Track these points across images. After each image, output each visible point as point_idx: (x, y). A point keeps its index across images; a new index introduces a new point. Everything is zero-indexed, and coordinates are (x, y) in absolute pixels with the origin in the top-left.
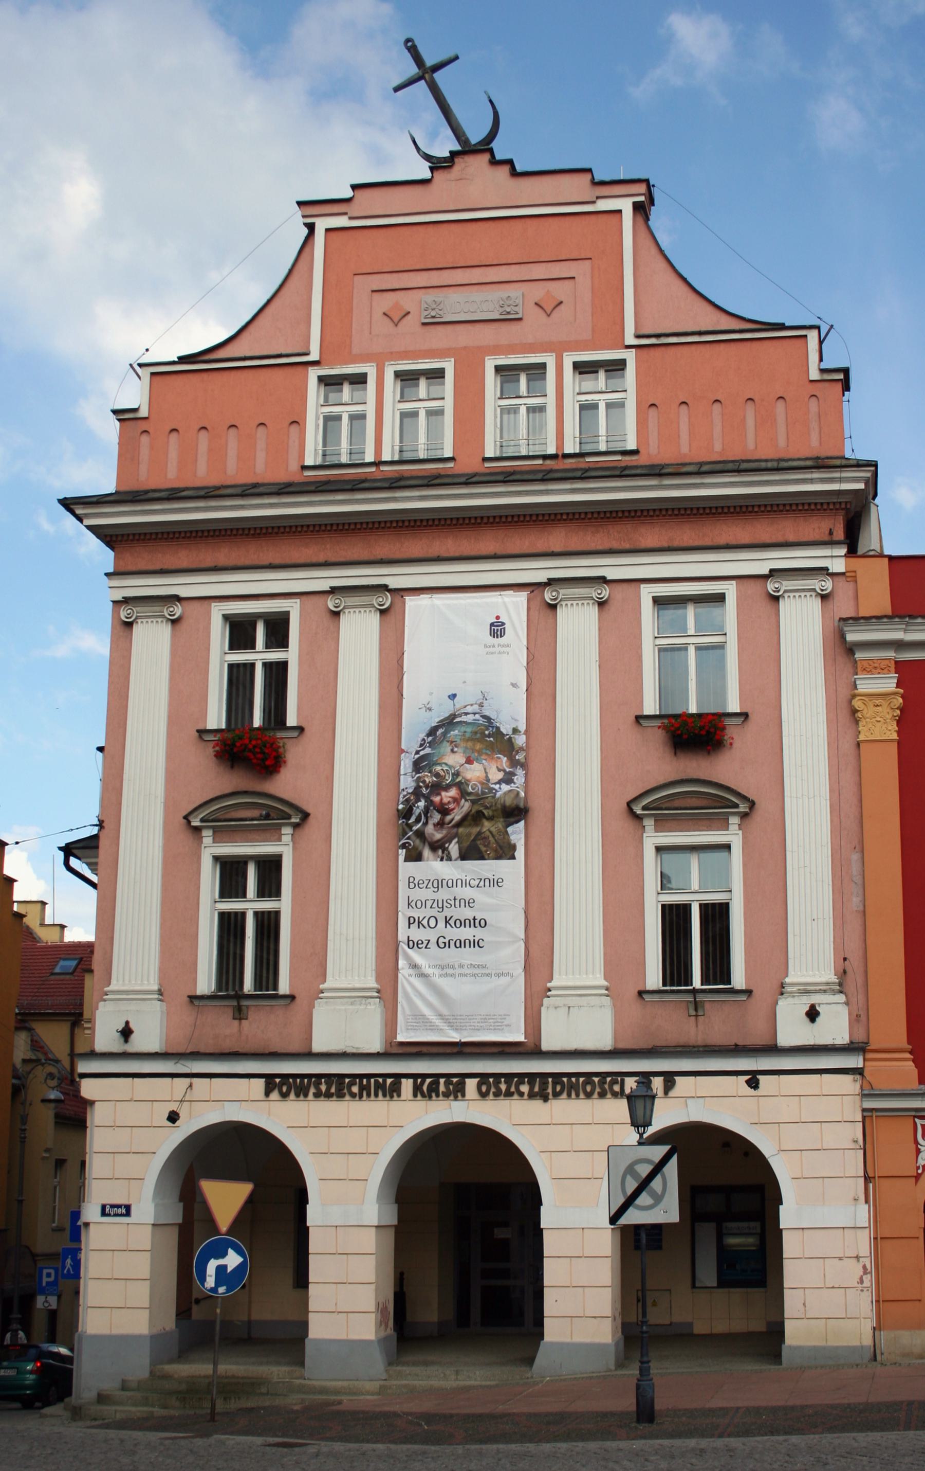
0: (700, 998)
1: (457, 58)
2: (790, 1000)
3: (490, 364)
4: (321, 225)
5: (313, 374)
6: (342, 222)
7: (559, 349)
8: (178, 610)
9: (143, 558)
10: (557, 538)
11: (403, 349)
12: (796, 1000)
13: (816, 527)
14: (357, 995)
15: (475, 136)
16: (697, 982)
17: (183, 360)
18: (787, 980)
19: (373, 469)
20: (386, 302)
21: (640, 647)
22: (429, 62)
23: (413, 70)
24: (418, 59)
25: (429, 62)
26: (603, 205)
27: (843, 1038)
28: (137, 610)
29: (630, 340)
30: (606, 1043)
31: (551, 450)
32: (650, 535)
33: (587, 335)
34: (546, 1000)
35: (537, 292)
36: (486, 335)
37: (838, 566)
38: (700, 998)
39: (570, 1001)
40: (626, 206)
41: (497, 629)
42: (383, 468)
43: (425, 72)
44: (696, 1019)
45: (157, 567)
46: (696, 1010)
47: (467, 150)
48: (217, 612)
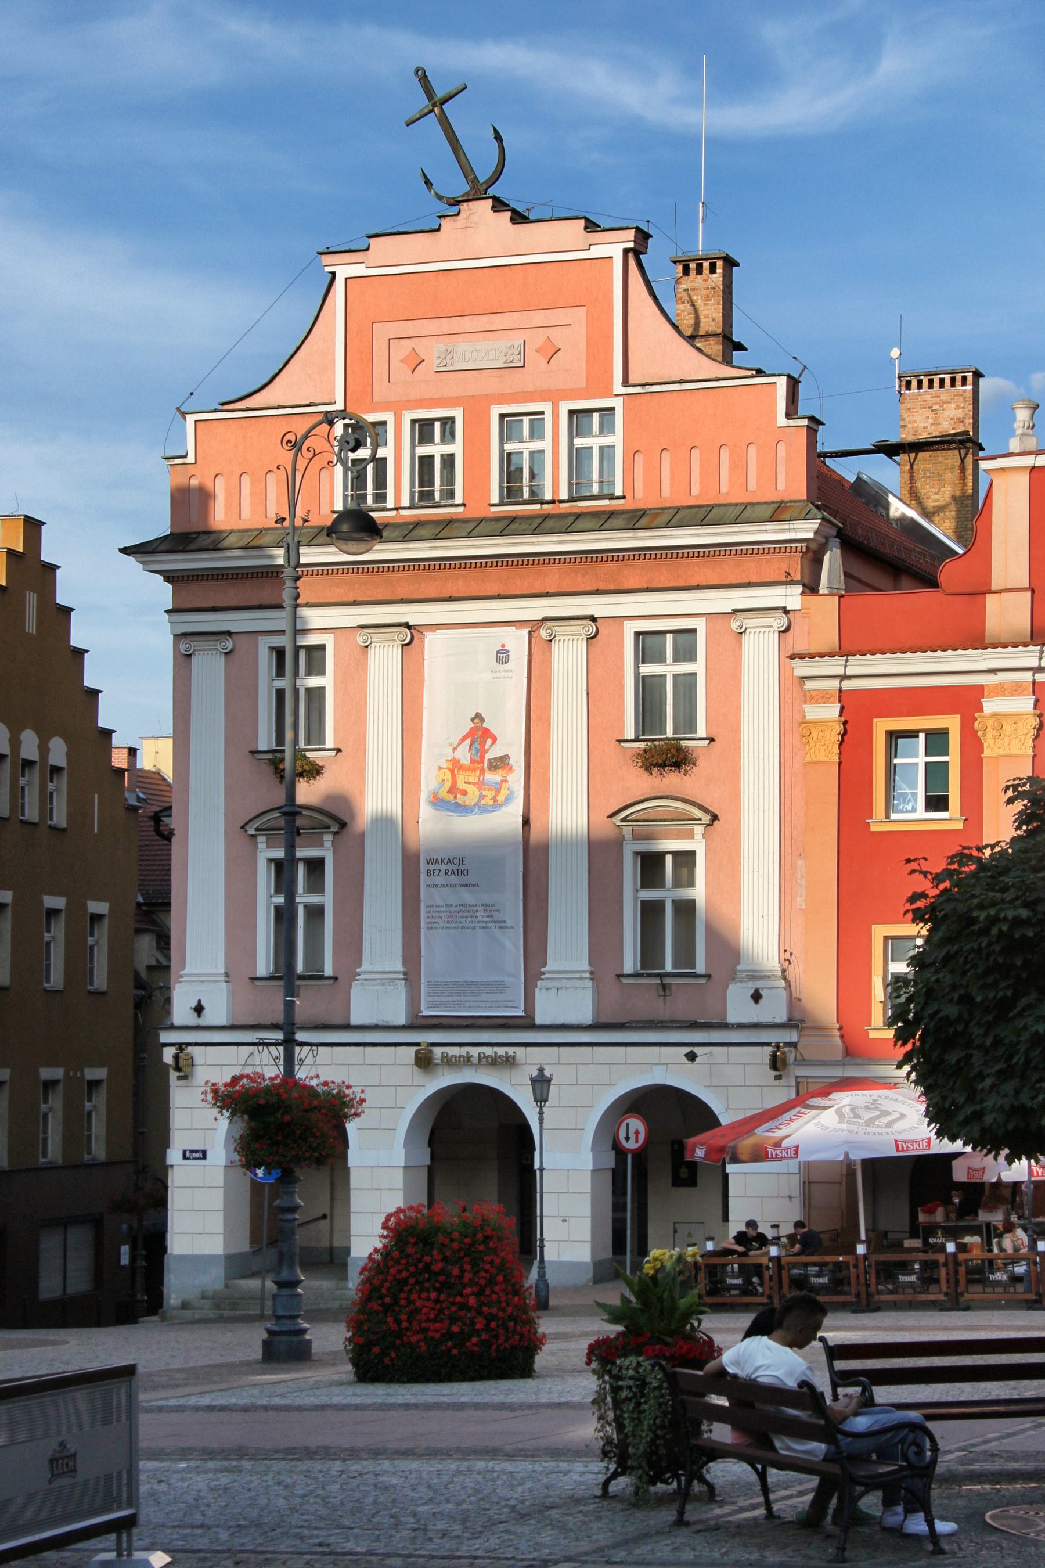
0: (667, 980)
1: (465, 88)
2: (739, 985)
3: (496, 411)
4: (342, 272)
8: (229, 645)
9: (199, 594)
10: (553, 577)
11: (418, 397)
12: (743, 985)
14: (384, 978)
15: (483, 172)
16: (669, 968)
17: (225, 404)
18: (739, 967)
19: (394, 513)
21: (622, 677)
22: (440, 93)
23: (424, 102)
24: (429, 91)
25: (440, 93)
27: (782, 1017)
28: (196, 644)
30: (587, 1018)
31: (548, 496)
32: (633, 577)
33: (582, 383)
34: (539, 983)
38: (667, 980)
39: (558, 984)
42: (402, 512)
43: (434, 105)
44: (665, 1000)
45: (210, 604)
46: (664, 991)
47: (477, 192)
48: (264, 644)
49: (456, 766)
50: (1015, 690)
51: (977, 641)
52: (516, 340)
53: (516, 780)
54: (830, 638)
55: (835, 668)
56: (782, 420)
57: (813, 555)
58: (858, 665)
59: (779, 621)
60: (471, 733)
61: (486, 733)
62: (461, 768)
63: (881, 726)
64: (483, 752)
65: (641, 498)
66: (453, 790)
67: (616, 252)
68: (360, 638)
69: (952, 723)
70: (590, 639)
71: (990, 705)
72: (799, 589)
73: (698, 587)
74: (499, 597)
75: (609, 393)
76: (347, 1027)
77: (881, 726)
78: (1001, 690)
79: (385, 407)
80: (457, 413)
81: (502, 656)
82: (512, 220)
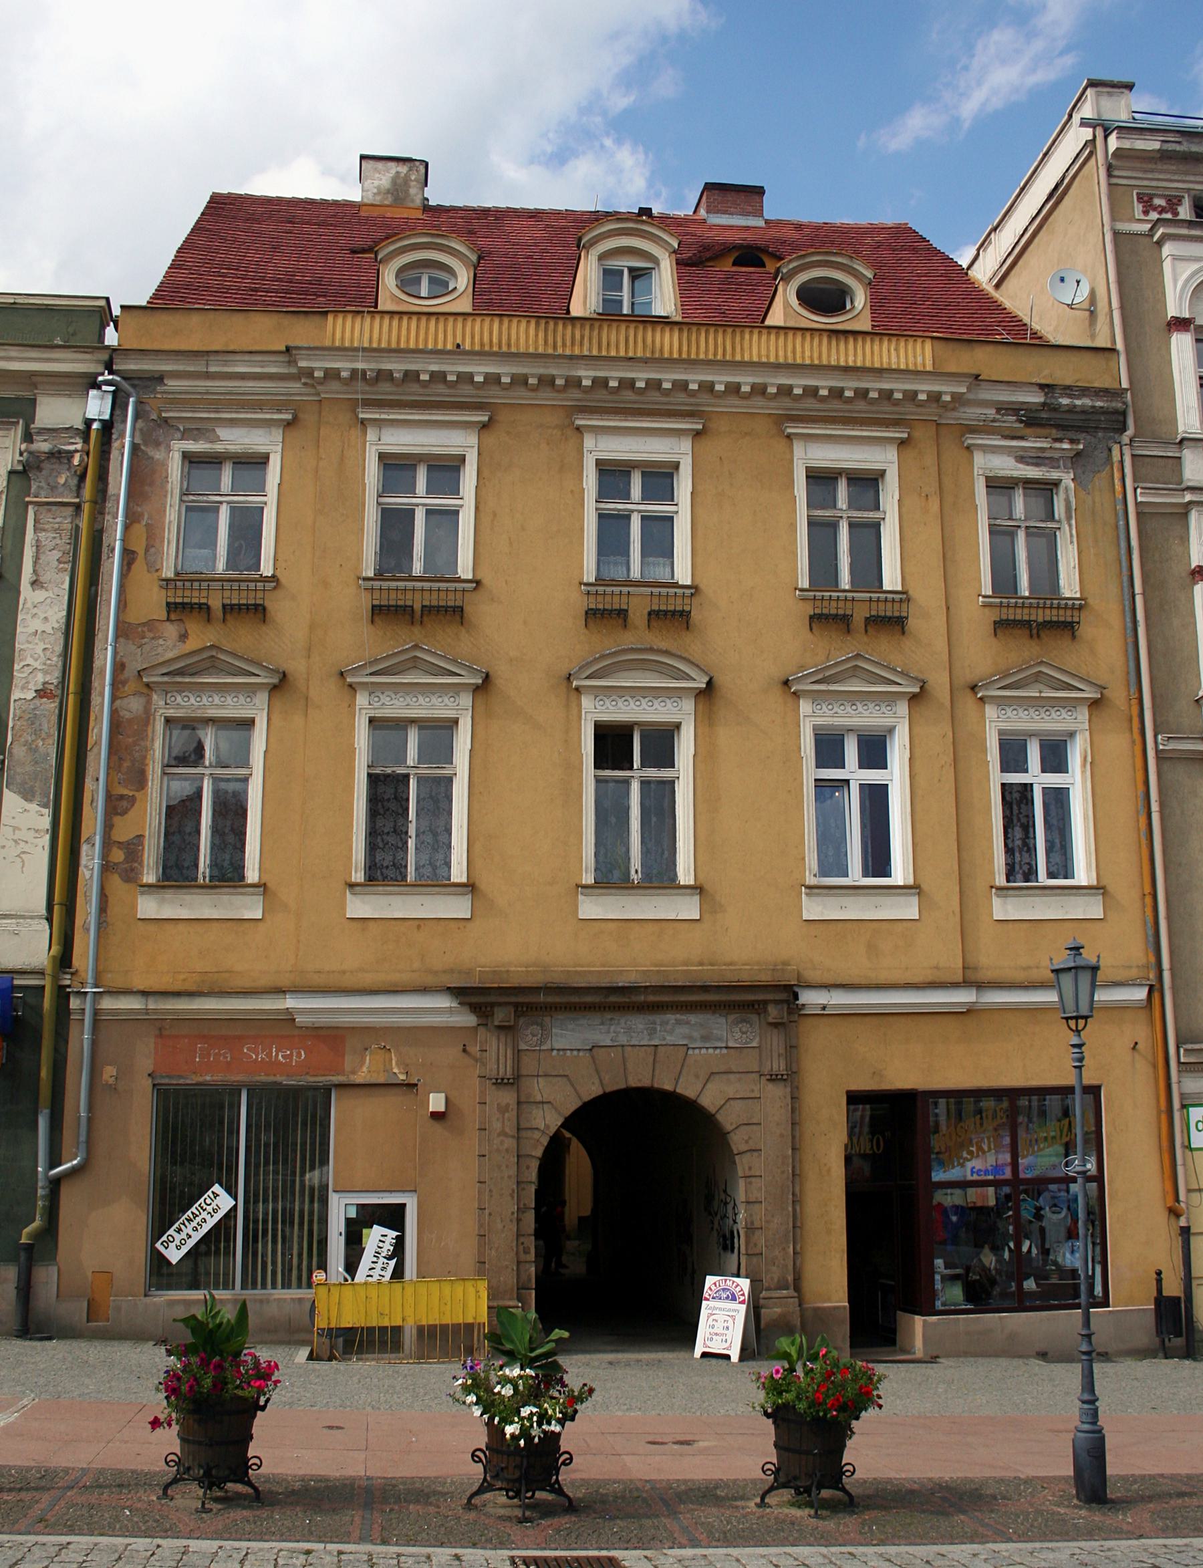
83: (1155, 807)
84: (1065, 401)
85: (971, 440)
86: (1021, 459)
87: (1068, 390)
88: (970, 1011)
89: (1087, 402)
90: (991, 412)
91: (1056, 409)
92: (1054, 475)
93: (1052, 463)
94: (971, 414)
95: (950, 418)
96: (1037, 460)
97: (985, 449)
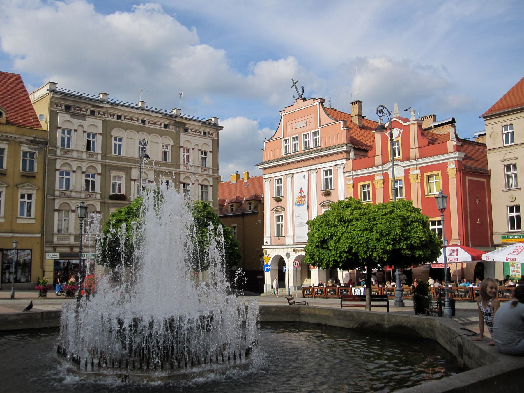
5: (283, 139)
6: (284, 114)
7: (310, 130)
10: (311, 162)
13: (341, 156)
20: (290, 126)
26: (315, 104)
29: (319, 127)
35: (308, 120)
36: (302, 129)
37: (345, 162)
40: (317, 103)
41: (304, 177)
49: (298, 198)
50: (379, 175)
51: (373, 166)
52: (305, 121)
53: (306, 199)
54: (351, 169)
55: (350, 174)
56: (342, 129)
57: (348, 153)
58: (355, 173)
59: (343, 166)
60: (300, 192)
61: (303, 192)
62: (299, 198)
63: (360, 184)
64: (302, 194)
65: (323, 146)
66: (298, 202)
67: (318, 103)
68: (286, 176)
69: (370, 182)
70: (317, 173)
71: (376, 178)
72: (346, 160)
73: (331, 161)
74: (304, 167)
75: (317, 128)
76: (285, 245)
77: (360, 184)
78: (378, 175)
79: (288, 136)
80: (298, 135)
81: (304, 177)
82: (304, 101)
83: (45, 207)
84: (37, 140)
85: (21, 144)
86: (29, 148)
87: (38, 138)
88: (12, 237)
89: (41, 140)
90: (25, 140)
91: (36, 141)
92: (35, 151)
93: (35, 149)
94: (21, 140)
95: (18, 140)
96: (32, 149)
97: (23, 146)
